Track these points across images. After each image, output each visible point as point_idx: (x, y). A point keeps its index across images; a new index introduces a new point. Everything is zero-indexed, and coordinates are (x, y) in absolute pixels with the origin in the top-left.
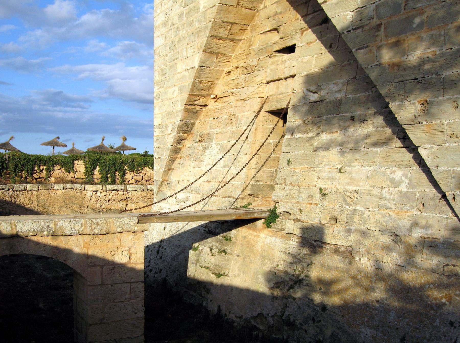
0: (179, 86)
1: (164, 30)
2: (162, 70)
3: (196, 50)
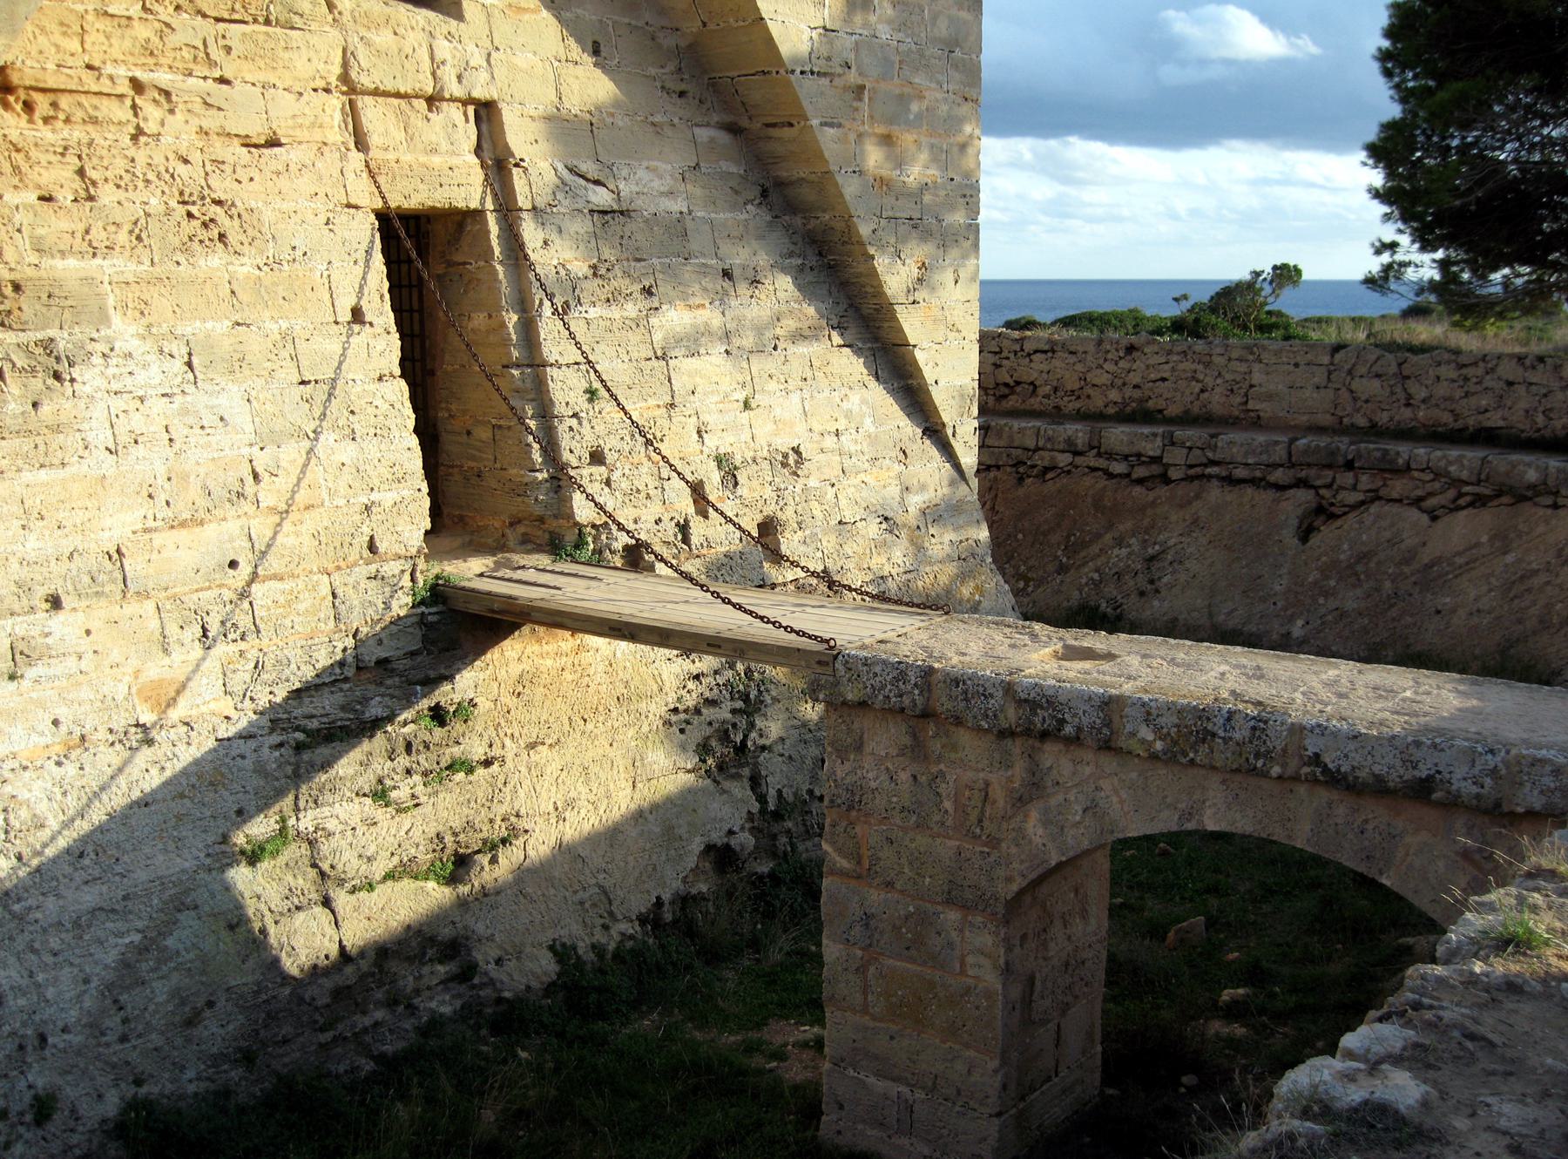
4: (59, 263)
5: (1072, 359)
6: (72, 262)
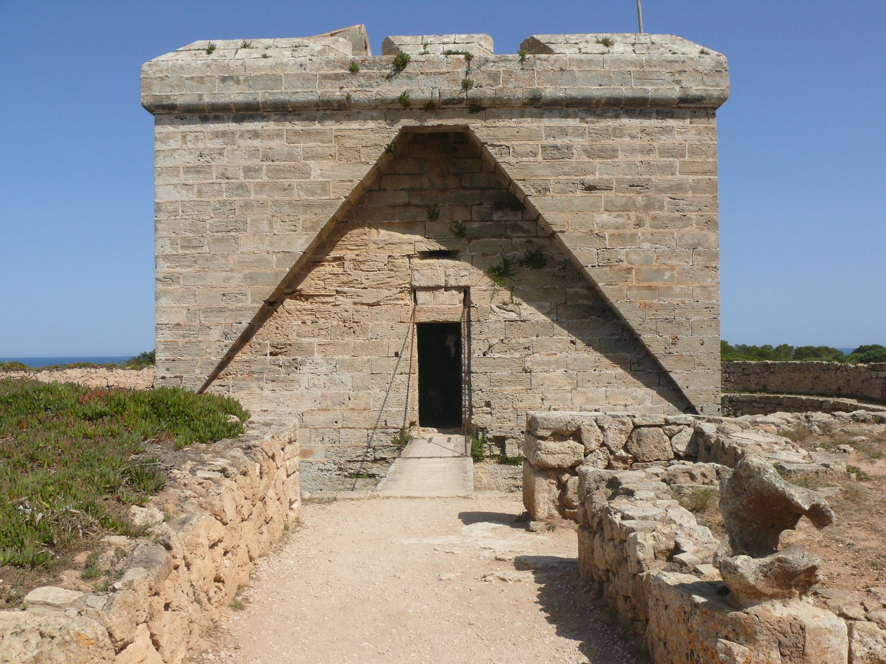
0: (246, 271)
1: (191, 179)
2: (185, 239)
3: (300, 228)
4: (303, 339)
6: (307, 339)
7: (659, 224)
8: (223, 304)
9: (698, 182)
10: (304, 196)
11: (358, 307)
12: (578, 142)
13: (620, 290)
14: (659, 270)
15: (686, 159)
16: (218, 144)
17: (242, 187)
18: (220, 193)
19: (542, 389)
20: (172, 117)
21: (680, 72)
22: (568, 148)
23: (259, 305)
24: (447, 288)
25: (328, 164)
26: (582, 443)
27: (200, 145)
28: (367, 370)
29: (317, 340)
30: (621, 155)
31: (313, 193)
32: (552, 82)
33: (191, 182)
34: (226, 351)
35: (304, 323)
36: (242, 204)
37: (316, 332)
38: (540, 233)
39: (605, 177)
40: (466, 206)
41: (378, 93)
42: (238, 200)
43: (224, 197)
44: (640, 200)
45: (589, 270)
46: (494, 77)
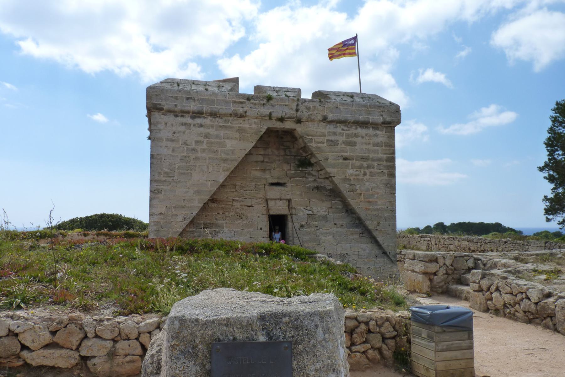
1: (169, 144)
2: (165, 173)
3: (221, 170)
5: (495, 245)
7: (372, 174)
8: (183, 204)
9: (388, 158)
10: (224, 156)
11: (243, 207)
12: (341, 139)
13: (357, 202)
14: (372, 194)
15: (383, 148)
16: (183, 128)
17: (194, 149)
18: (183, 151)
19: (324, 244)
20: (160, 114)
21: (382, 111)
22: (338, 141)
23: (202, 205)
24: (281, 199)
25: (234, 142)
26: (438, 263)
27: (174, 129)
28: (248, 236)
29: (225, 222)
30: (357, 144)
31: (228, 154)
32: (332, 112)
33: (169, 145)
34: (184, 226)
35: (218, 214)
36: (194, 157)
37: (224, 218)
38: (320, 177)
39: (351, 154)
40: (288, 163)
41: (259, 112)
42: (192, 156)
43: (185, 154)
44: (365, 164)
45: (344, 193)
46: (308, 108)
